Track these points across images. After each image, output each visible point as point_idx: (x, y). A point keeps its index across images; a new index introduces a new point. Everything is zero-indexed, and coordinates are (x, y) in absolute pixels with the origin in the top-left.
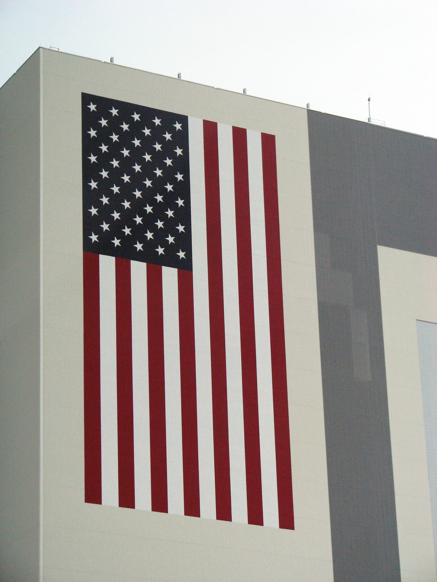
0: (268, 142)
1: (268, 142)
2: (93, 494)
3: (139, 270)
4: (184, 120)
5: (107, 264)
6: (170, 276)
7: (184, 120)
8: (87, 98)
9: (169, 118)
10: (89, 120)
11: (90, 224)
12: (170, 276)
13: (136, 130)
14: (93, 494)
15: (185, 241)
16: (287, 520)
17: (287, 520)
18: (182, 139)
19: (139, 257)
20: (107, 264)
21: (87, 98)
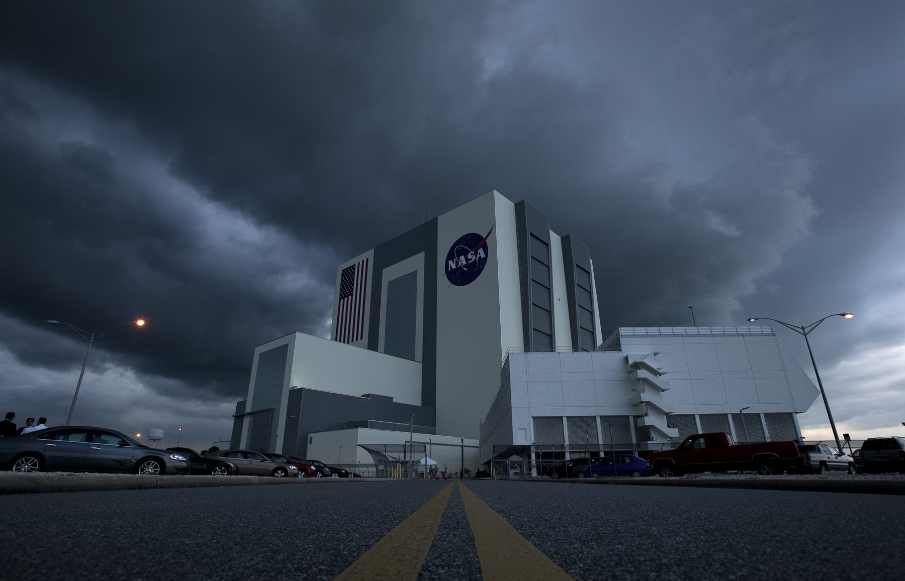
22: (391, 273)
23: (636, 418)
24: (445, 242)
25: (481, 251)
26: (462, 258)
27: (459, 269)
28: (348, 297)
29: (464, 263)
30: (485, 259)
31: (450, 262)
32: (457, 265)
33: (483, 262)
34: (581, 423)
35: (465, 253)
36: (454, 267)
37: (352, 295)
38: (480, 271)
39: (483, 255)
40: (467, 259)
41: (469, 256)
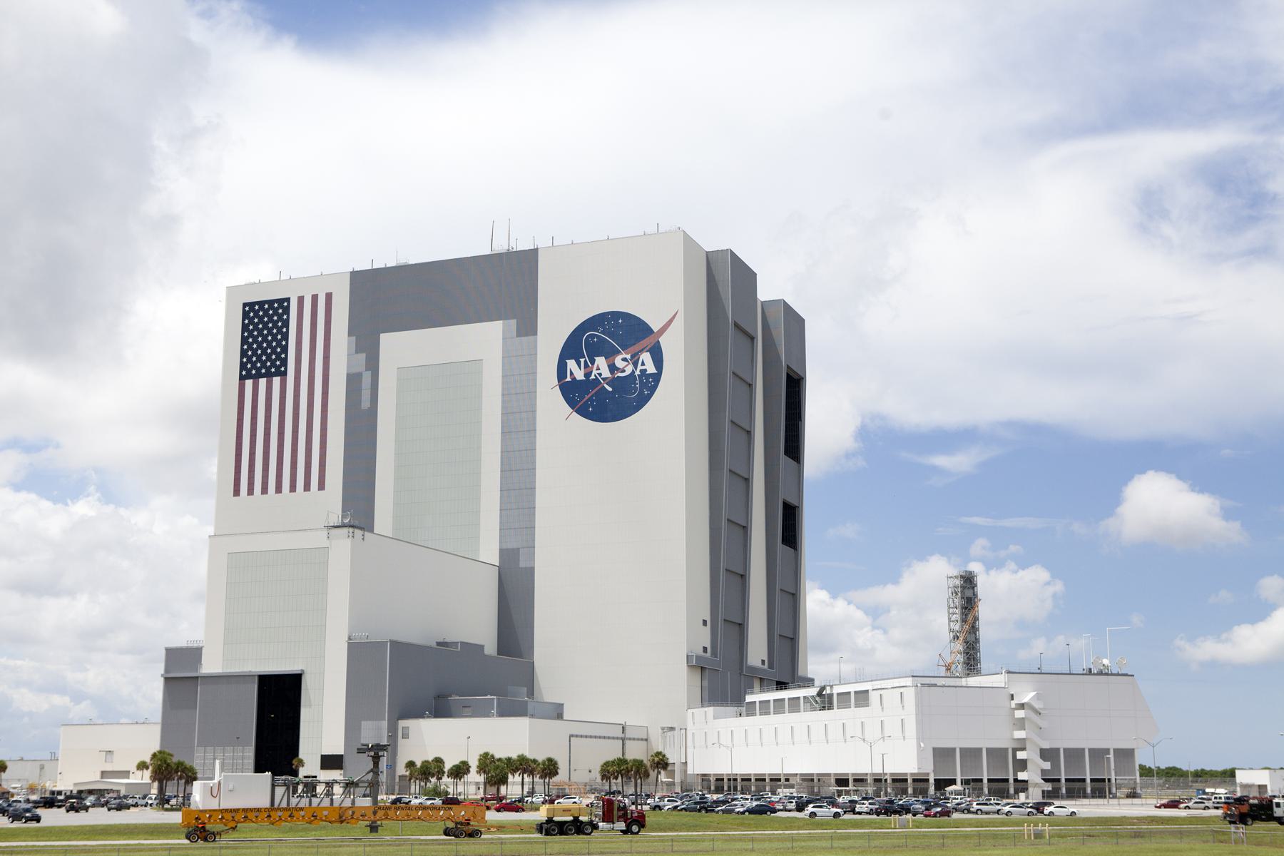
0: (329, 297)
1: (329, 297)
2: (237, 492)
4: (288, 300)
5: (249, 383)
7: (288, 300)
8: (245, 305)
9: (281, 301)
10: (245, 315)
11: (243, 366)
13: (266, 312)
14: (237, 492)
15: (284, 362)
16: (322, 486)
17: (322, 486)
19: (263, 376)
21: (245, 305)
22: (401, 349)
23: (1015, 750)
24: (558, 319)
25: (646, 357)
26: (601, 361)
27: (590, 383)
29: (606, 373)
30: (657, 377)
31: (571, 364)
32: (588, 375)
33: (650, 383)
34: (971, 755)
35: (610, 354)
36: (580, 375)
37: (285, 373)
39: (651, 369)
40: (613, 368)
41: (619, 362)
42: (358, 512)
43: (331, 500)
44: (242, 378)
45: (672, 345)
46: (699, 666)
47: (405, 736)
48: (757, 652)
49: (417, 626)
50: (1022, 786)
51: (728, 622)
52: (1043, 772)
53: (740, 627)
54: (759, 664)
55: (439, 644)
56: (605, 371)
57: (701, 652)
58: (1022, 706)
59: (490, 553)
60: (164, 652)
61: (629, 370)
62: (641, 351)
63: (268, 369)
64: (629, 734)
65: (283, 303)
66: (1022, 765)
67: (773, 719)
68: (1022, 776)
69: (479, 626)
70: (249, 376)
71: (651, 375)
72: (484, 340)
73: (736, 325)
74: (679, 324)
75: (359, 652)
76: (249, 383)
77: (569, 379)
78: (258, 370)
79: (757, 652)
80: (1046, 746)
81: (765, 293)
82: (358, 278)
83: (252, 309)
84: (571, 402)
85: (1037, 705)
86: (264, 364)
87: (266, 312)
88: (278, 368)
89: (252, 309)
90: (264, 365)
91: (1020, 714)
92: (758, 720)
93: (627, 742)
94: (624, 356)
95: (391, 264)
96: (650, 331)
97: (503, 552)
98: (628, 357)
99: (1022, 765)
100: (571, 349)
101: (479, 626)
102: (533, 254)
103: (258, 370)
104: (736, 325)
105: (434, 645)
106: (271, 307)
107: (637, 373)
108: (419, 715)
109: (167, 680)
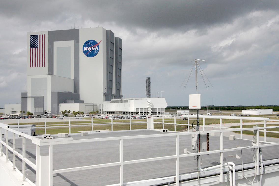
0: (45, 35)
1: (45, 35)
2: (30, 67)
3: (34, 49)
6: (36, 49)
7: (38, 35)
8: (30, 36)
9: (36, 35)
10: (30, 37)
12: (36, 49)
13: (34, 37)
14: (30, 67)
16: (45, 66)
17: (45, 66)
18: (38, 37)
20: (32, 49)
23: (148, 108)
25: (97, 47)
26: (89, 48)
28: (35, 48)
29: (90, 50)
30: (98, 50)
31: (85, 48)
32: (88, 50)
33: (97, 51)
35: (91, 46)
36: (86, 50)
37: (38, 48)
38: (96, 54)
39: (97, 49)
40: (91, 49)
41: (92, 48)
42: (51, 71)
43: (46, 68)
44: (30, 48)
45: (101, 45)
46: (105, 95)
47: (60, 106)
48: (114, 92)
49: (62, 90)
50: (148, 113)
51: (109, 88)
52: (151, 111)
53: (111, 88)
54: (114, 94)
55: (65, 92)
56: (91, 47)
57: (105, 93)
58: (149, 102)
59: (72, 77)
60: (21, 93)
61: (94, 50)
62: (96, 46)
63: (35, 47)
64: (94, 105)
65: (37, 36)
66: (148, 110)
67: (115, 104)
68: (148, 112)
69: (71, 89)
70: (32, 48)
71: (98, 50)
72: (71, 44)
73: (111, 42)
74: (102, 42)
75: (52, 93)
76: (32, 49)
77: (84, 50)
78: (33, 47)
79: (114, 92)
80: (152, 108)
81: (116, 36)
82: (49, 32)
83: (32, 37)
84: (85, 54)
85: (151, 102)
86: (34, 46)
87: (34, 37)
88: (37, 47)
89: (32, 37)
90: (34, 46)
91: (148, 103)
92: (113, 104)
93: (94, 106)
94: (93, 47)
95: (55, 30)
96: (97, 43)
97: (74, 77)
98: (94, 47)
99: (148, 110)
100: (85, 45)
101: (71, 89)
102: (78, 30)
103: (33, 47)
104: (111, 42)
105: (64, 92)
106: (35, 36)
107: (95, 50)
108: (62, 103)
109: (22, 97)
